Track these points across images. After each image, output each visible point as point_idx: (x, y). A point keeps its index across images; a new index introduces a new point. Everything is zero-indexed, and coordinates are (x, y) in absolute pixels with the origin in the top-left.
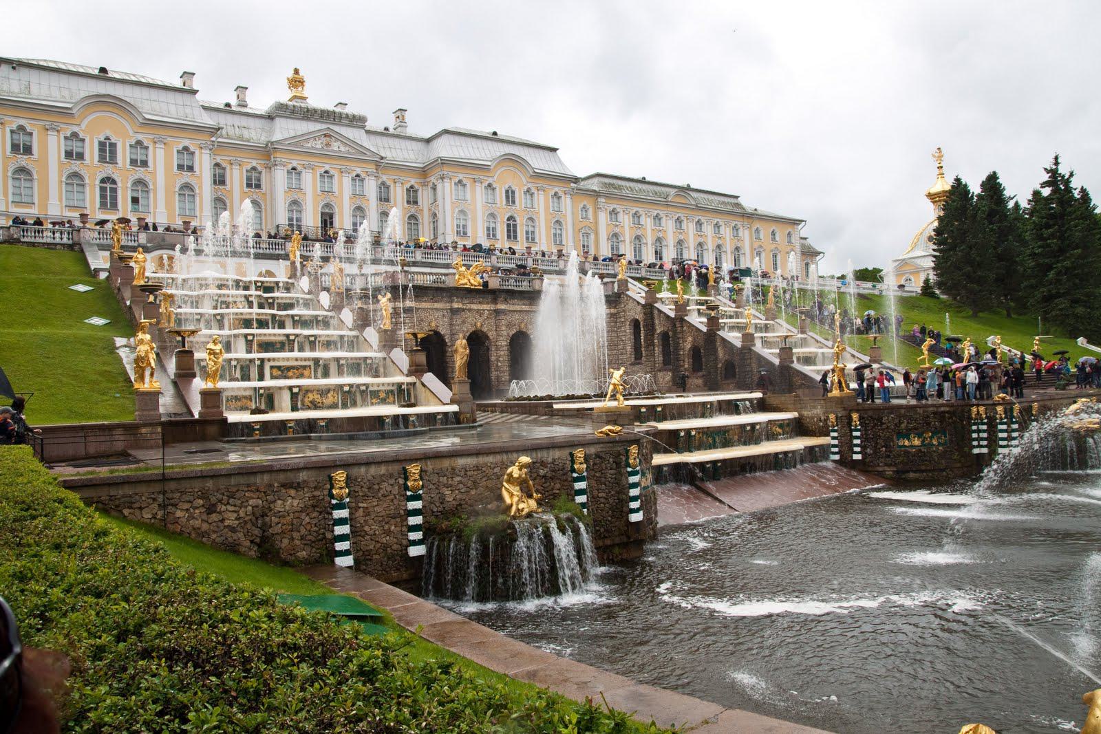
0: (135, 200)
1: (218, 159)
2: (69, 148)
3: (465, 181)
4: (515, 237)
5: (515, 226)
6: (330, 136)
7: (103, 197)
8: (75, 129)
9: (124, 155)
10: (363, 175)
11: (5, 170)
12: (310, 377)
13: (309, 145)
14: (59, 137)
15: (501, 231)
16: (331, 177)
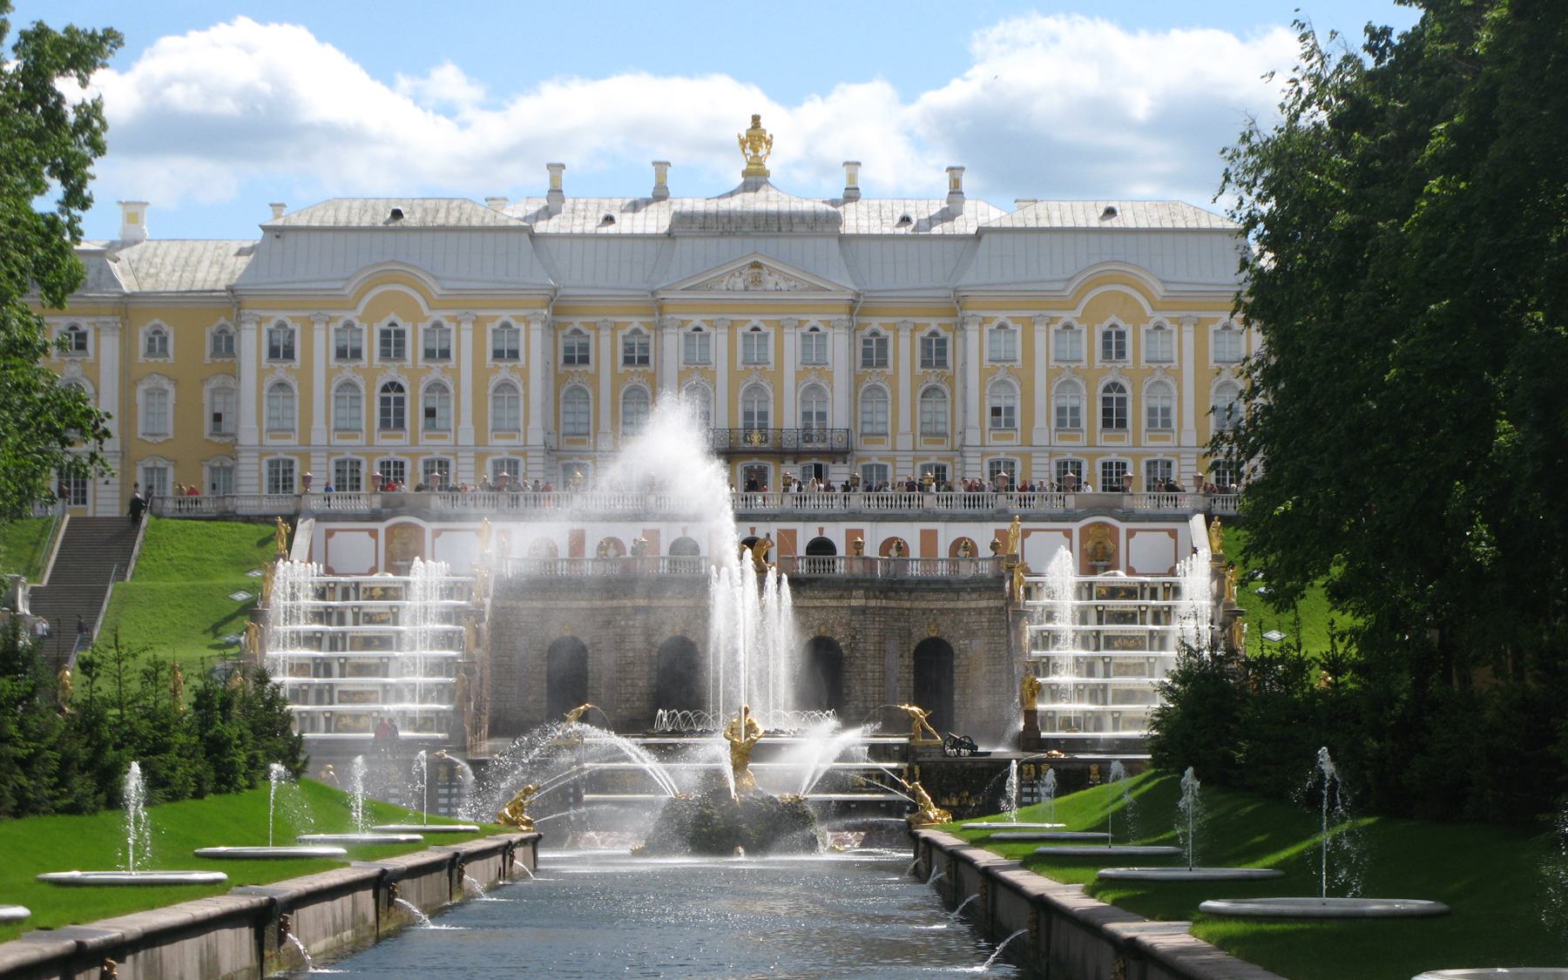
0: (430, 413)
1: (577, 325)
2: (341, 344)
3: (1011, 326)
4: (1122, 424)
5: (1122, 402)
6: (756, 265)
7: (385, 412)
8: (349, 316)
9: (414, 346)
10: (822, 328)
11: (260, 388)
12: (376, 701)
13: (723, 286)
14: (327, 330)
15: (1092, 413)
16: (766, 335)
